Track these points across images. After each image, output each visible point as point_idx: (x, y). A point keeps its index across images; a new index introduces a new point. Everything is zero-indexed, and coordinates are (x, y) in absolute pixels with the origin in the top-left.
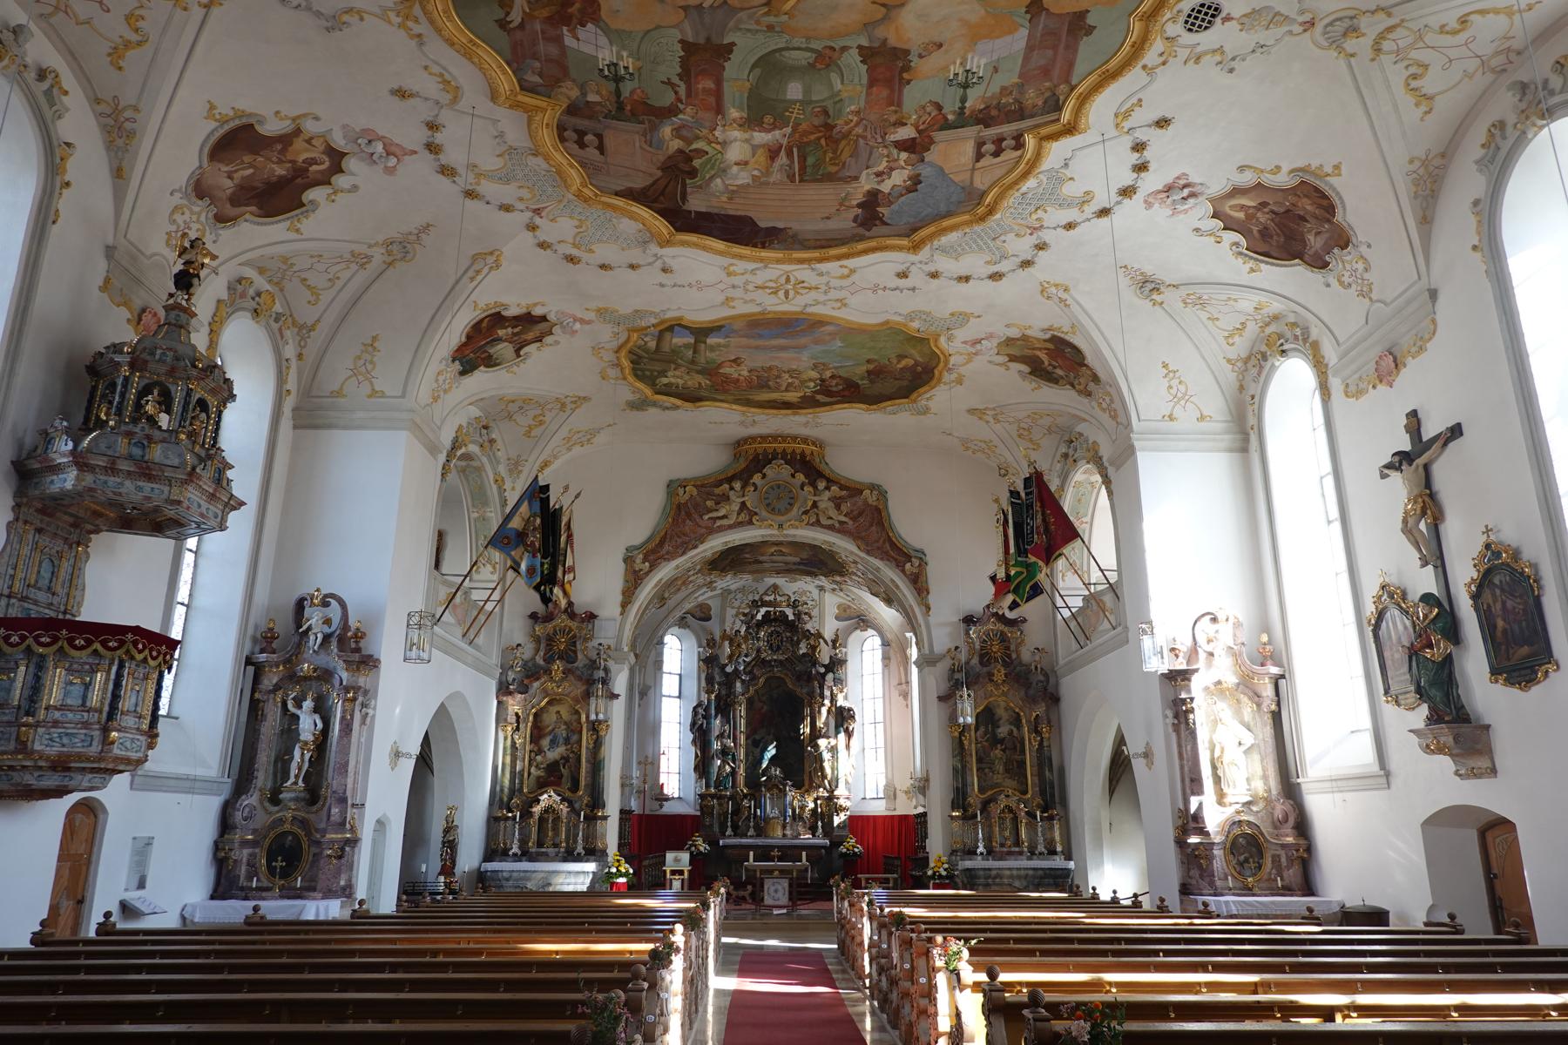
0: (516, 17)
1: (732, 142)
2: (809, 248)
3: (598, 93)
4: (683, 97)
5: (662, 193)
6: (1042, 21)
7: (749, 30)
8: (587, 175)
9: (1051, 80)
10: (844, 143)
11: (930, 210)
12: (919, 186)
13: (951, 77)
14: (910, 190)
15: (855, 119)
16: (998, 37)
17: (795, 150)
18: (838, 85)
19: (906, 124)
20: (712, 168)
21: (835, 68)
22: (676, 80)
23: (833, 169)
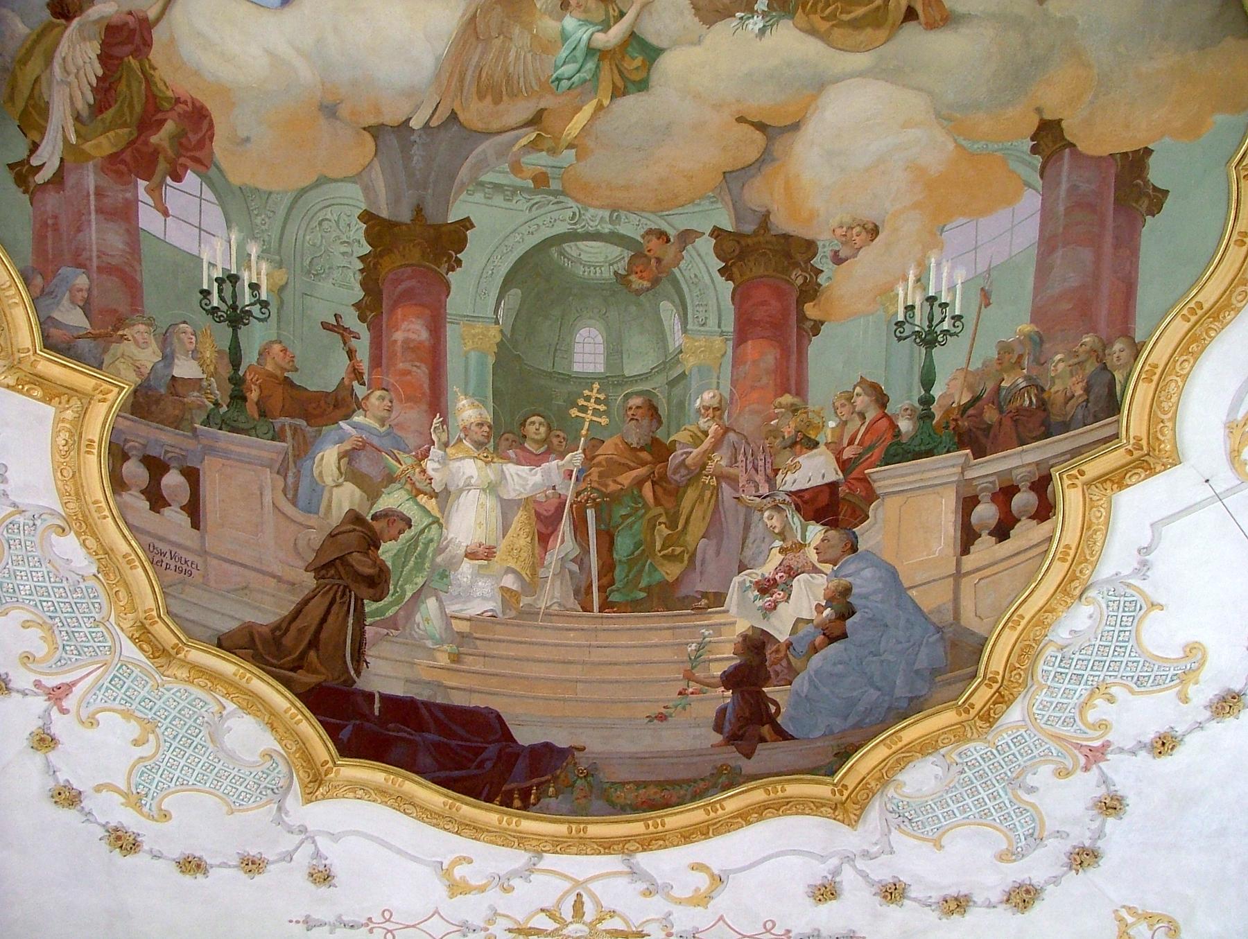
0: (49, 157)
1: (461, 491)
2: (623, 810)
3: (196, 354)
4: (365, 366)
5: (314, 643)
6: (1066, 167)
7: (497, 187)
8: (162, 588)
9: (1093, 329)
10: (691, 494)
11: (873, 694)
12: (849, 622)
13: (901, 318)
14: (834, 634)
16: (984, 212)
17: (590, 514)
18: (677, 339)
19: (816, 445)
20: (419, 567)
22: (351, 320)
23: (671, 571)
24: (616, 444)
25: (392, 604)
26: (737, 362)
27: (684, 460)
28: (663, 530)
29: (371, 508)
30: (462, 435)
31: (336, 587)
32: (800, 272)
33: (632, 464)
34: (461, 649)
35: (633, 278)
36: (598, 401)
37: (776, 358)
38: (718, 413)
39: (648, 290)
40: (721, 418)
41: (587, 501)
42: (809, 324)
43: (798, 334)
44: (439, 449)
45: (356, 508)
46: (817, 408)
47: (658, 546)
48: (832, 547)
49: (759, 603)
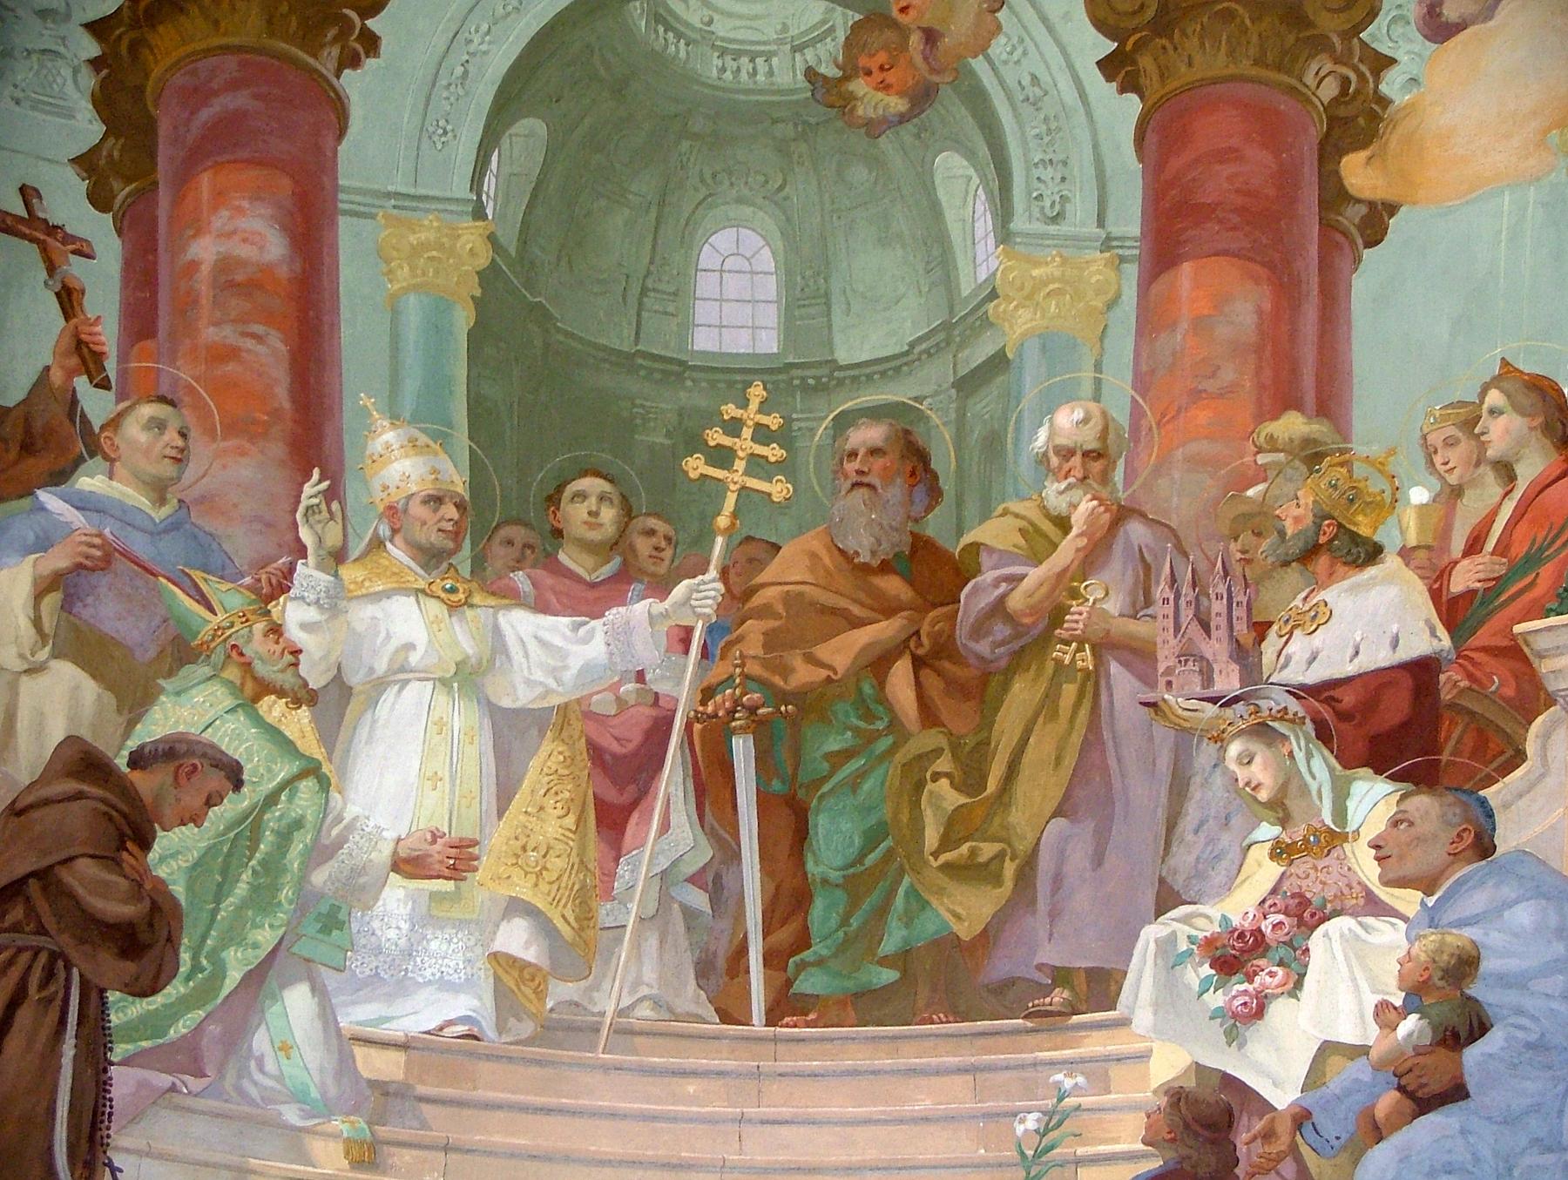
1: (380, 685)
4: (108, 335)
10: (1022, 694)
12: (1472, 1054)
15: (1084, 508)
17: (742, 749)
19: (1373, 553)
20: (263, 898)
21: (962, 115)
24: (814, 556)
25: (185, 1004)
26: (1151, 321)
27: (1002, 599)
28: (945, 796)
29: (127, 735)
30: (384, 531)
31: (25, 957)
32: (1329, 67)
33: (856, 610)
34: (383, 1131)
35: (859, 86)
36: (763, 435)
37: (1260, 312)
38: (1097, 466)
39: (903, 119)
40: (1105, 478)
41: (731, 713)
42: (1355, 213)
43: (1323, 235)
44: (319, 567)
45: (85, 733)
46: (1375, 450)
47: (931, 837)
48: (1419, 840)
49: (1216, 999)
